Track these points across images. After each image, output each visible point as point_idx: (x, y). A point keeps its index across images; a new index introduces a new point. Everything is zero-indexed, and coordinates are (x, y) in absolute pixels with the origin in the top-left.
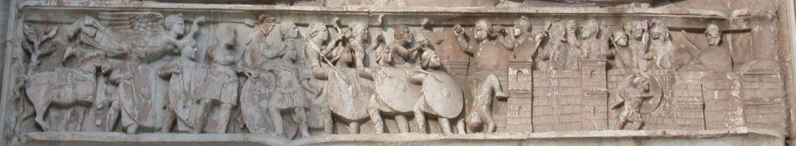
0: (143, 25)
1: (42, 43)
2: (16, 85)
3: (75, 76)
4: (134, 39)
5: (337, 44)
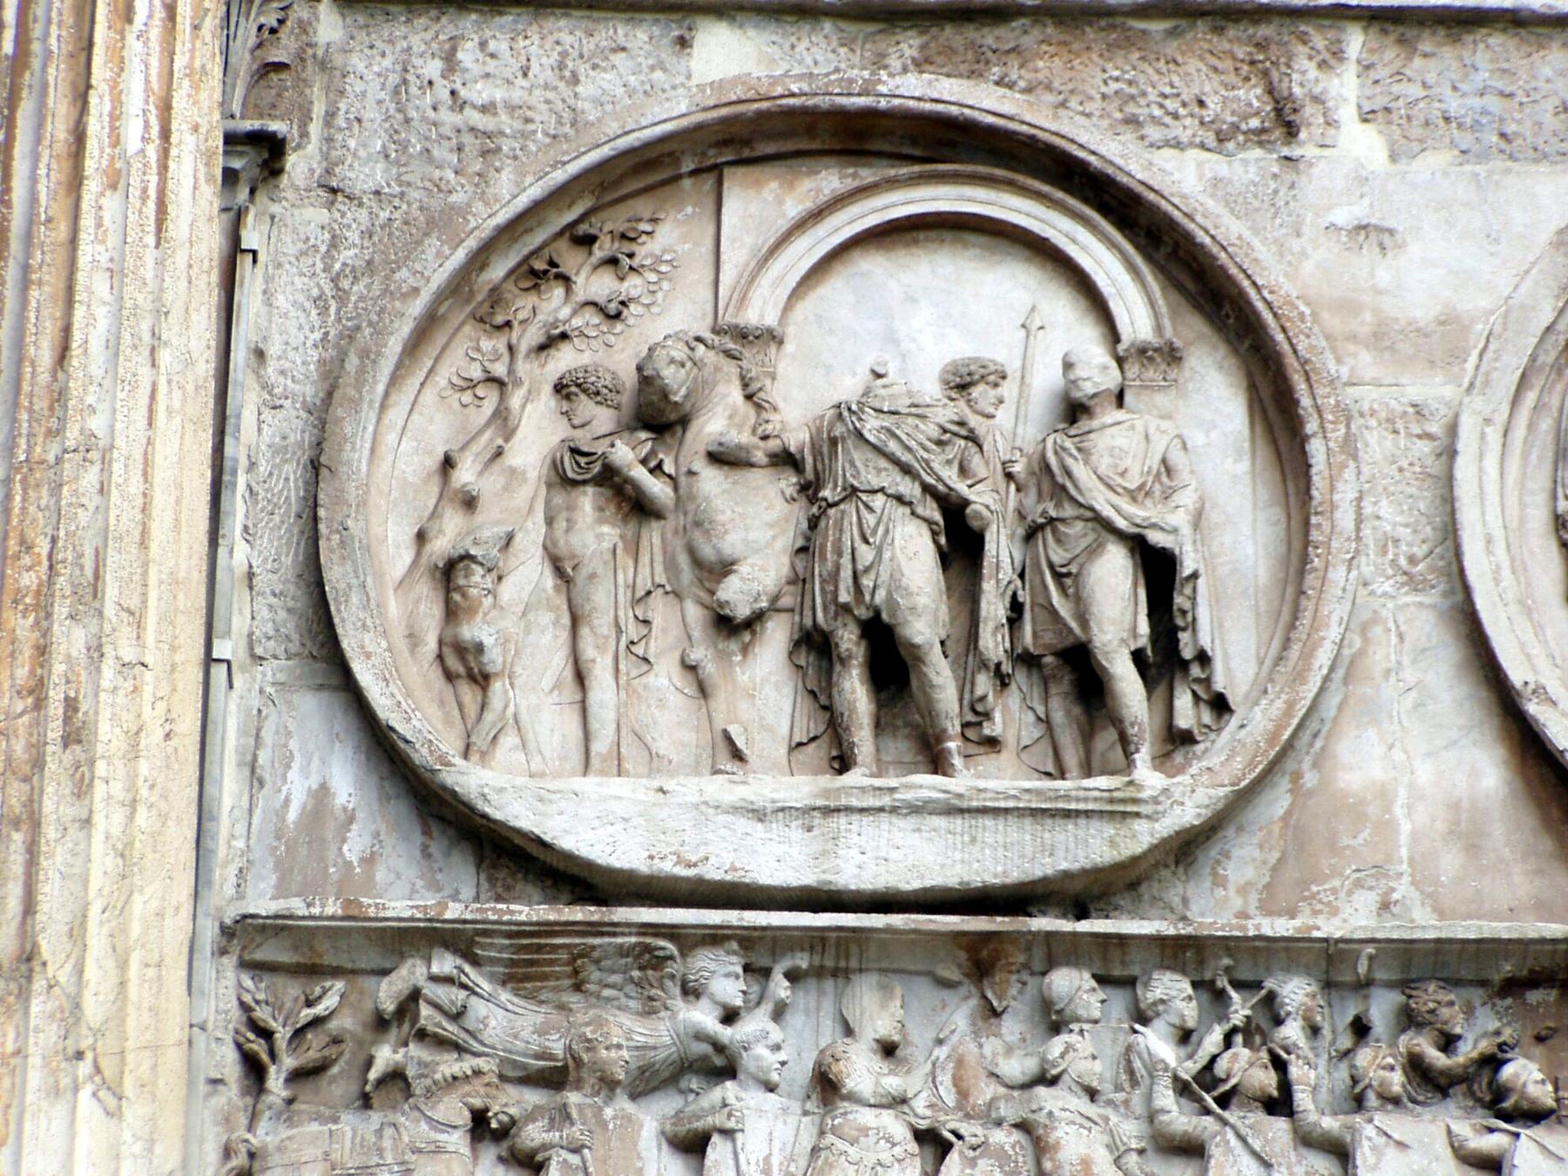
0: (616, 978)
1: (299, 1033)
2: (224, 1164)
3: (406, 1139)
4: (588, 1024)
5: (1228, 1041)
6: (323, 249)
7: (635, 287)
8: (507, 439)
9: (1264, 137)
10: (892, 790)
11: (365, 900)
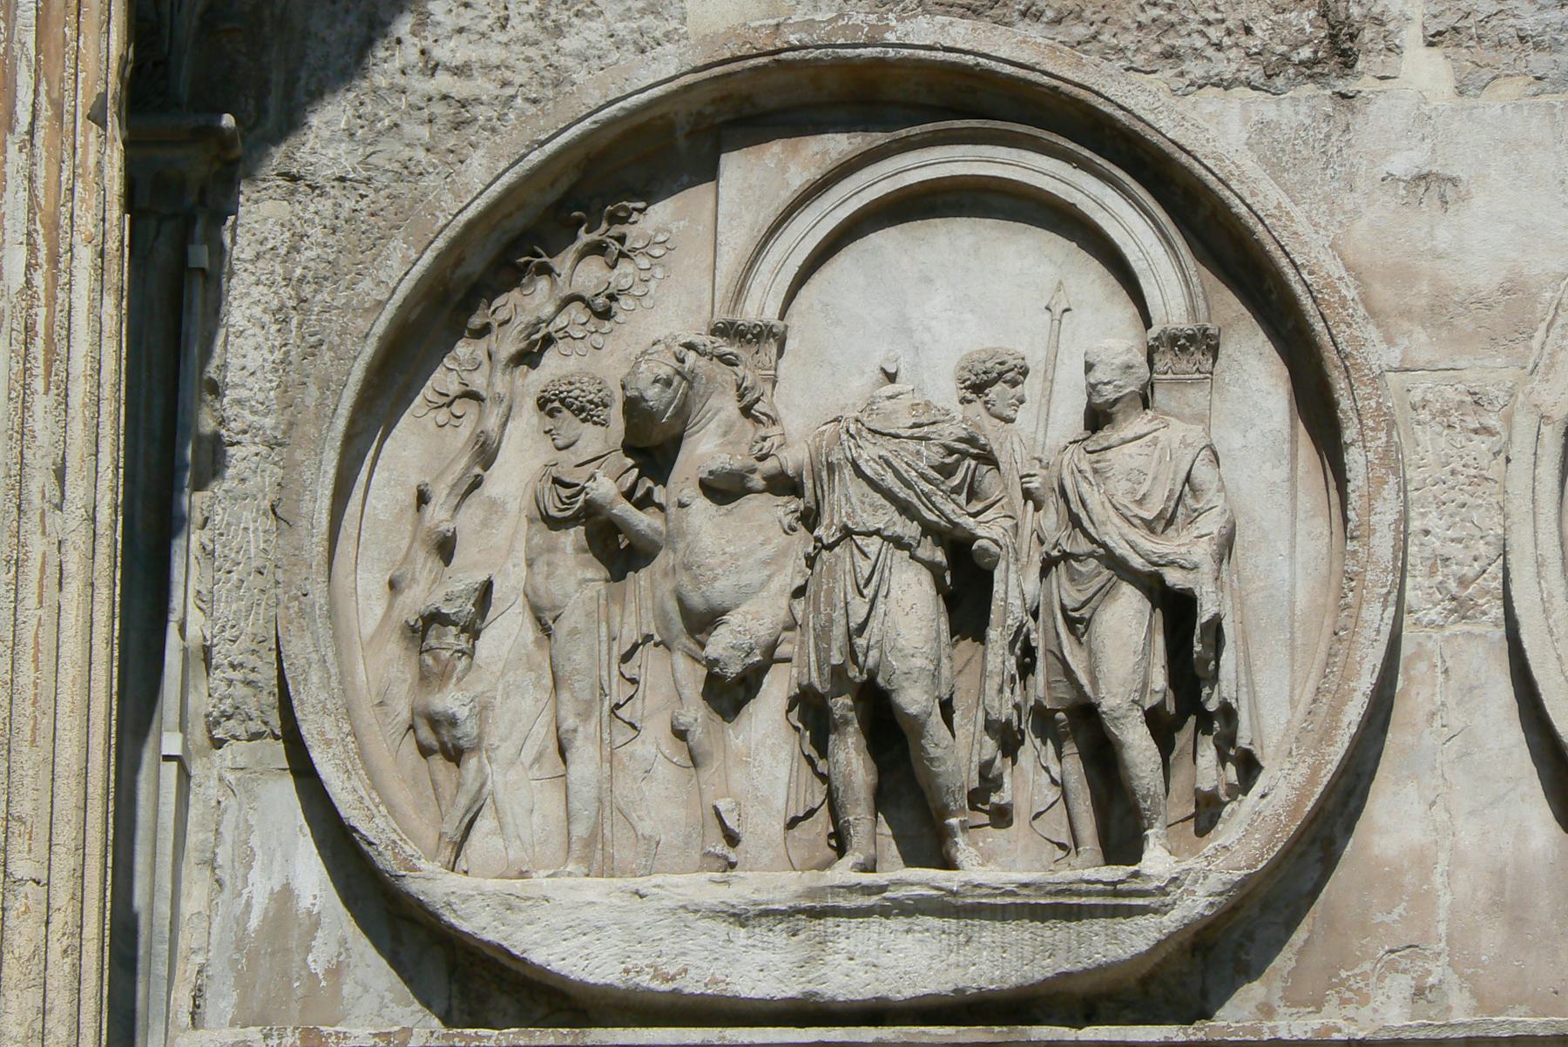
6: (283, 251)
7: (626, 276)
9: (1318, 69)
10: (882, 889)
11: (326, 1029)
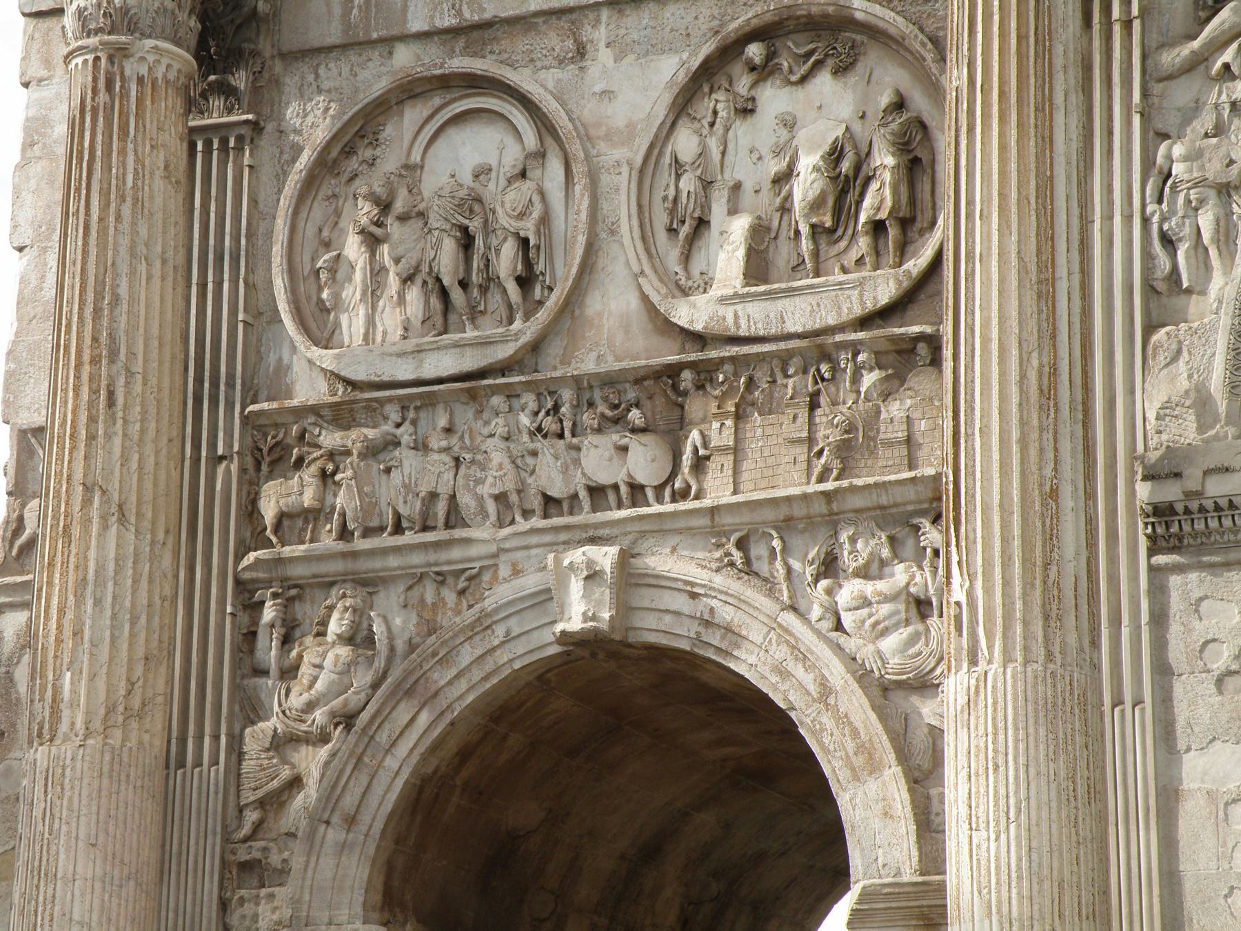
1: (271, 449)
5: (548, 414)
8: (339, 217)
